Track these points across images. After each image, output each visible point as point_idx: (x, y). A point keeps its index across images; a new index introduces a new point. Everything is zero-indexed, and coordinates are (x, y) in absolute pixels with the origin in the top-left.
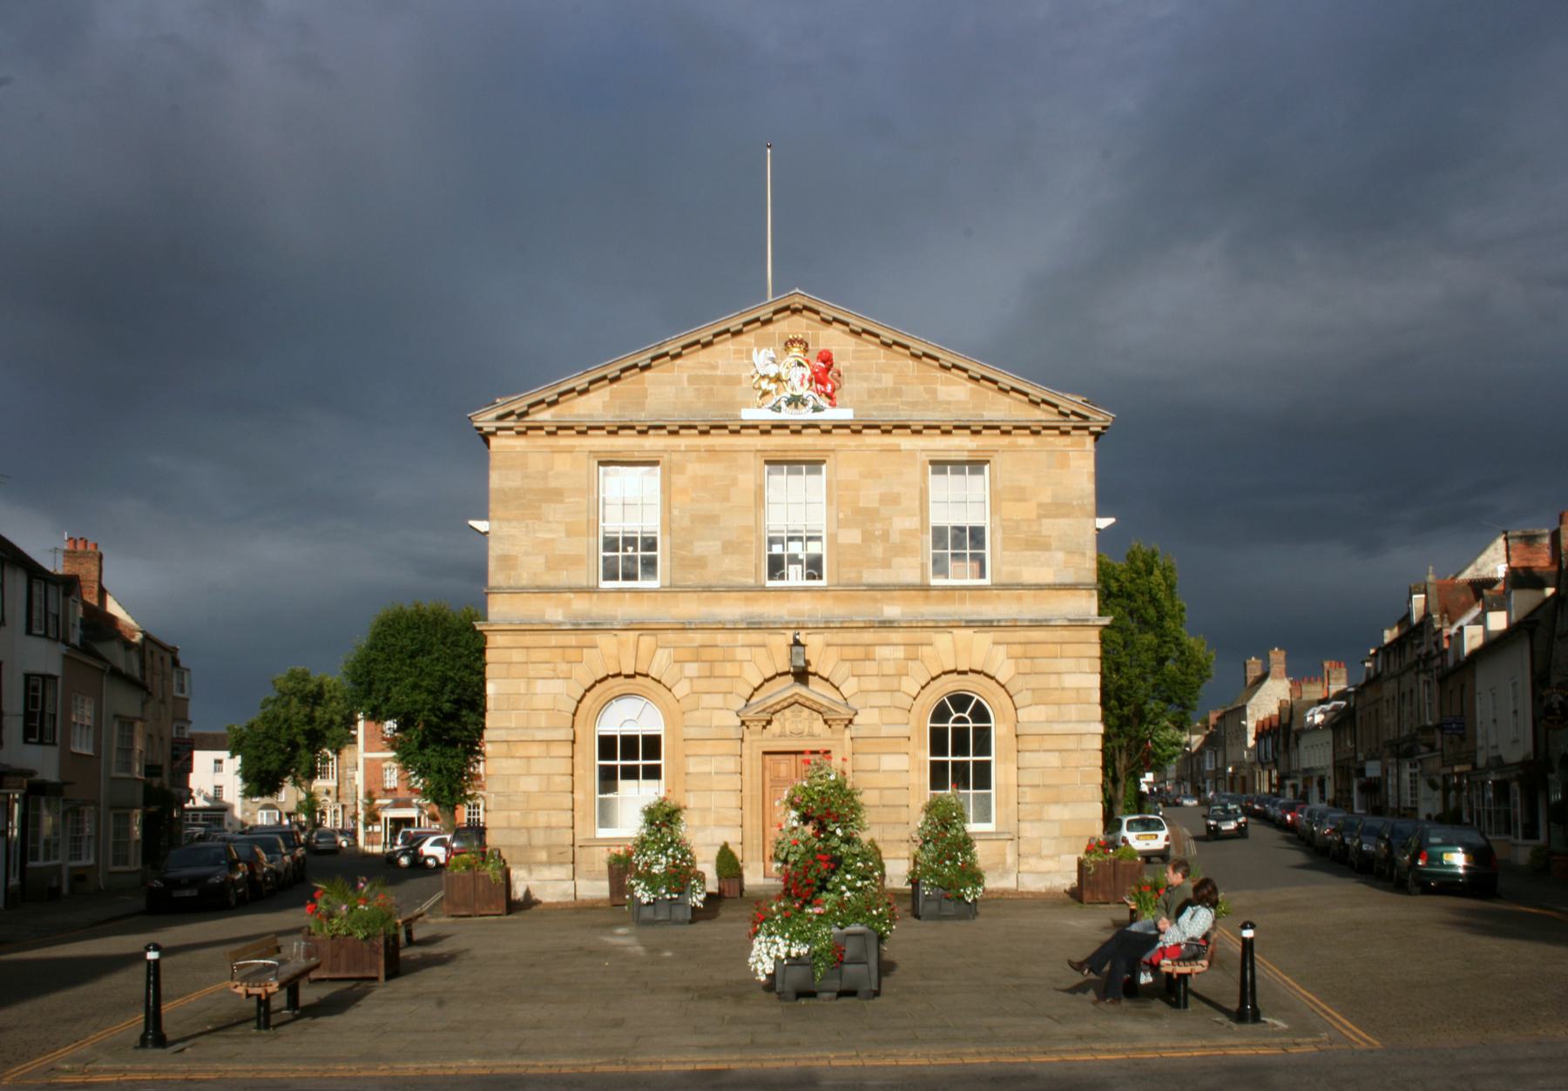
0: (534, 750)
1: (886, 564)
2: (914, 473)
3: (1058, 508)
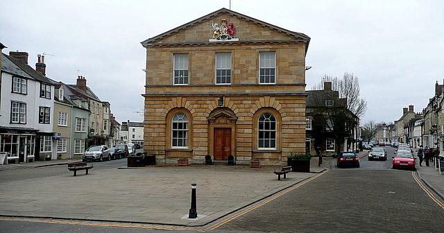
0: (156, 126)
2: (254, 55)
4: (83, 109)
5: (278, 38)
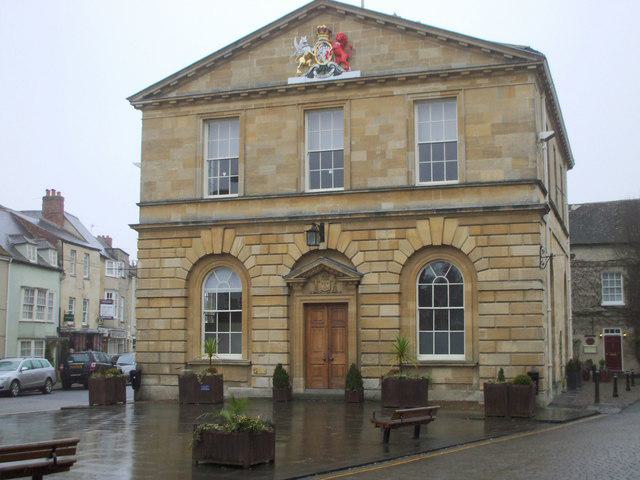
0: (163, 303)
1: (383, 173)
3: (507, 127)
4: (42, 267)
5: (461, 62)
